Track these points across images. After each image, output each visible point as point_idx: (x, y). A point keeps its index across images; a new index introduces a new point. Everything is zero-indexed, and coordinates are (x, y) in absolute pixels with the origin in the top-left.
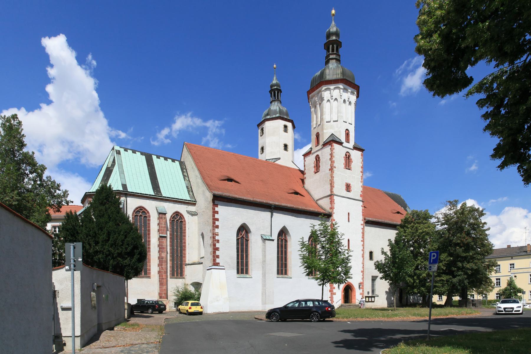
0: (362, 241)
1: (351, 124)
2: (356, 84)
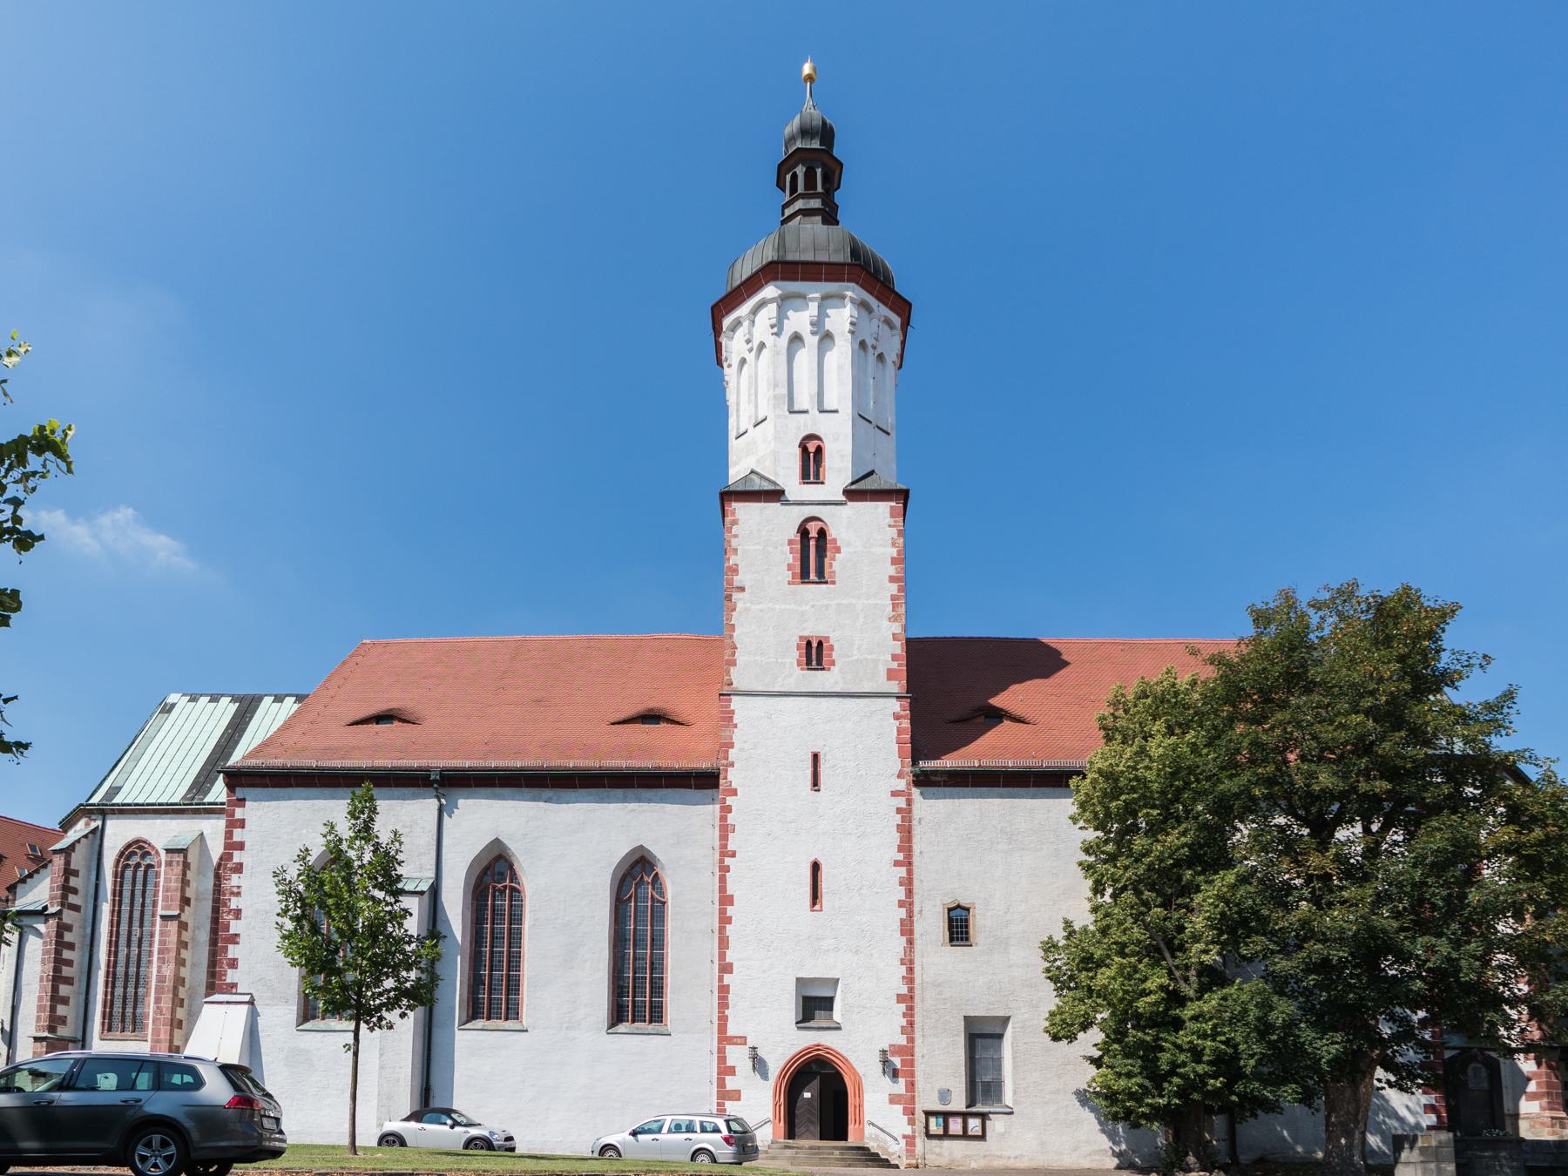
0: (897, 863)
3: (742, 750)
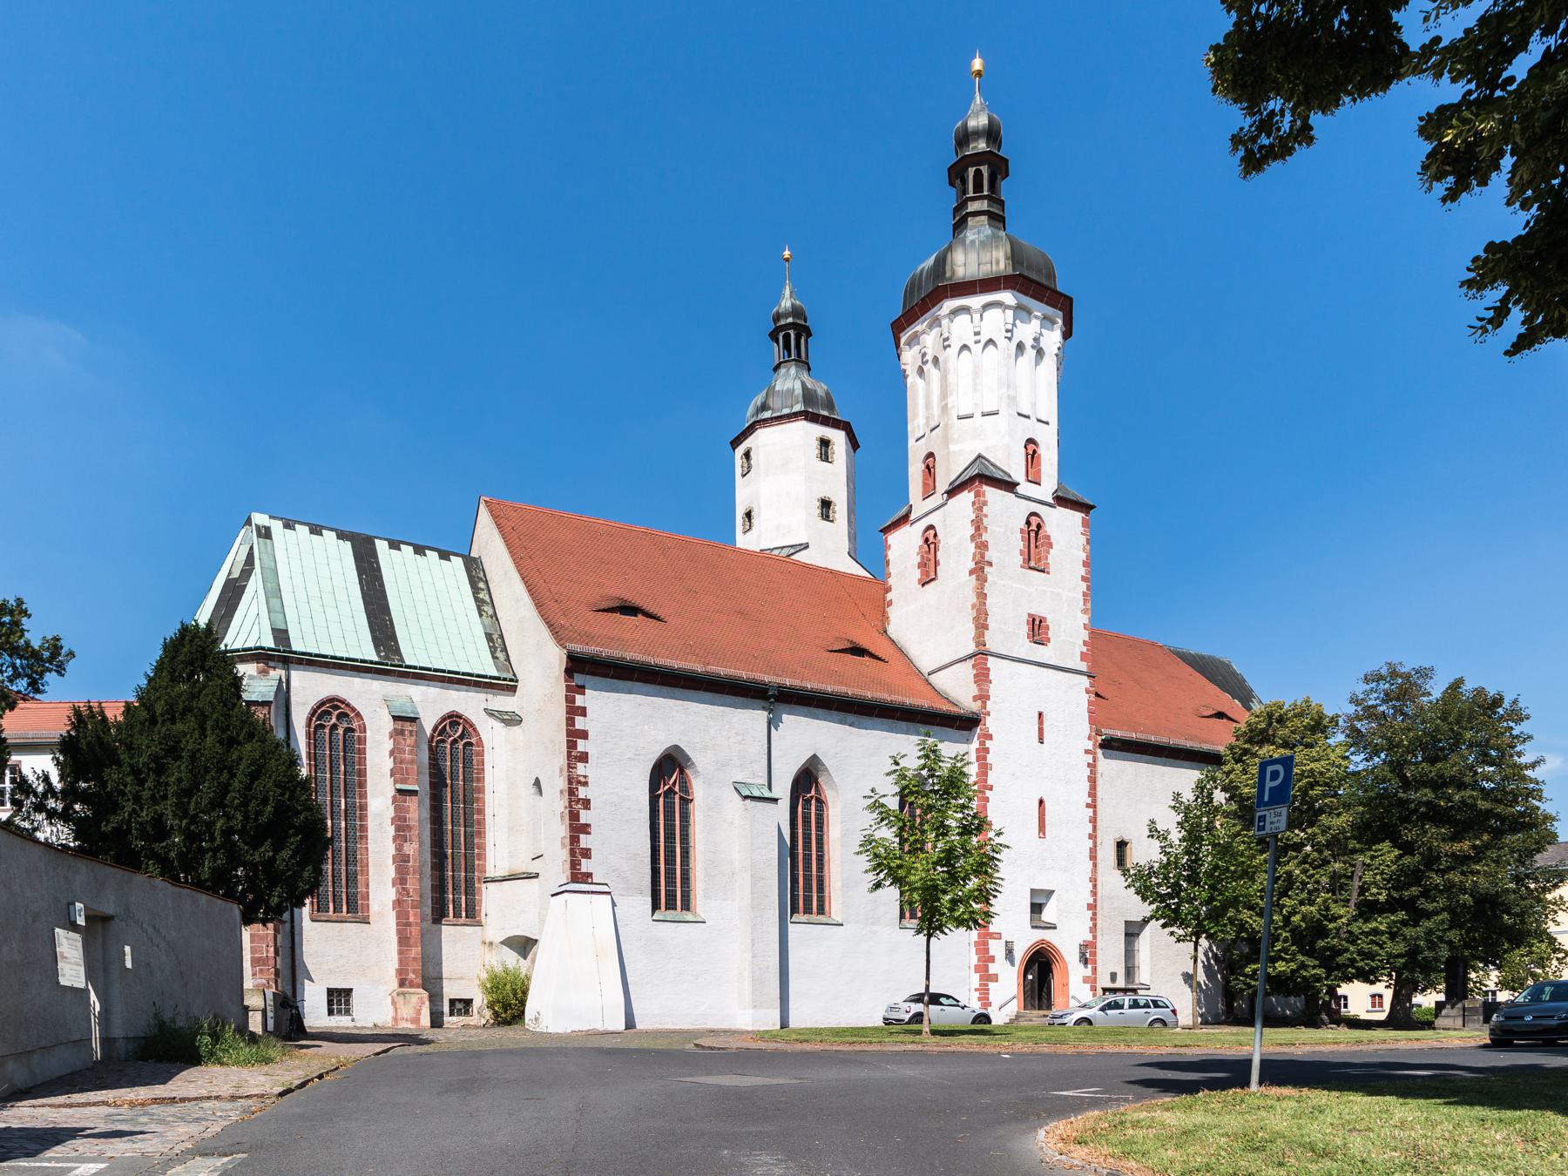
0: (1088, 806)
1: (1047, 423)
2: (1059, 289)
3: (994, 702)
